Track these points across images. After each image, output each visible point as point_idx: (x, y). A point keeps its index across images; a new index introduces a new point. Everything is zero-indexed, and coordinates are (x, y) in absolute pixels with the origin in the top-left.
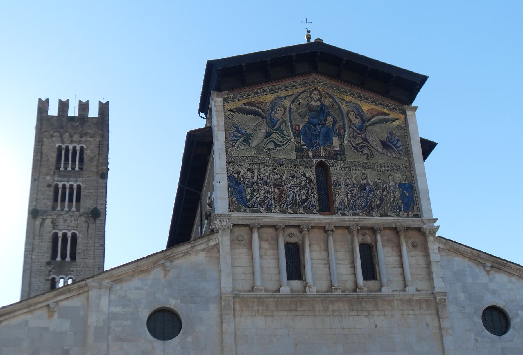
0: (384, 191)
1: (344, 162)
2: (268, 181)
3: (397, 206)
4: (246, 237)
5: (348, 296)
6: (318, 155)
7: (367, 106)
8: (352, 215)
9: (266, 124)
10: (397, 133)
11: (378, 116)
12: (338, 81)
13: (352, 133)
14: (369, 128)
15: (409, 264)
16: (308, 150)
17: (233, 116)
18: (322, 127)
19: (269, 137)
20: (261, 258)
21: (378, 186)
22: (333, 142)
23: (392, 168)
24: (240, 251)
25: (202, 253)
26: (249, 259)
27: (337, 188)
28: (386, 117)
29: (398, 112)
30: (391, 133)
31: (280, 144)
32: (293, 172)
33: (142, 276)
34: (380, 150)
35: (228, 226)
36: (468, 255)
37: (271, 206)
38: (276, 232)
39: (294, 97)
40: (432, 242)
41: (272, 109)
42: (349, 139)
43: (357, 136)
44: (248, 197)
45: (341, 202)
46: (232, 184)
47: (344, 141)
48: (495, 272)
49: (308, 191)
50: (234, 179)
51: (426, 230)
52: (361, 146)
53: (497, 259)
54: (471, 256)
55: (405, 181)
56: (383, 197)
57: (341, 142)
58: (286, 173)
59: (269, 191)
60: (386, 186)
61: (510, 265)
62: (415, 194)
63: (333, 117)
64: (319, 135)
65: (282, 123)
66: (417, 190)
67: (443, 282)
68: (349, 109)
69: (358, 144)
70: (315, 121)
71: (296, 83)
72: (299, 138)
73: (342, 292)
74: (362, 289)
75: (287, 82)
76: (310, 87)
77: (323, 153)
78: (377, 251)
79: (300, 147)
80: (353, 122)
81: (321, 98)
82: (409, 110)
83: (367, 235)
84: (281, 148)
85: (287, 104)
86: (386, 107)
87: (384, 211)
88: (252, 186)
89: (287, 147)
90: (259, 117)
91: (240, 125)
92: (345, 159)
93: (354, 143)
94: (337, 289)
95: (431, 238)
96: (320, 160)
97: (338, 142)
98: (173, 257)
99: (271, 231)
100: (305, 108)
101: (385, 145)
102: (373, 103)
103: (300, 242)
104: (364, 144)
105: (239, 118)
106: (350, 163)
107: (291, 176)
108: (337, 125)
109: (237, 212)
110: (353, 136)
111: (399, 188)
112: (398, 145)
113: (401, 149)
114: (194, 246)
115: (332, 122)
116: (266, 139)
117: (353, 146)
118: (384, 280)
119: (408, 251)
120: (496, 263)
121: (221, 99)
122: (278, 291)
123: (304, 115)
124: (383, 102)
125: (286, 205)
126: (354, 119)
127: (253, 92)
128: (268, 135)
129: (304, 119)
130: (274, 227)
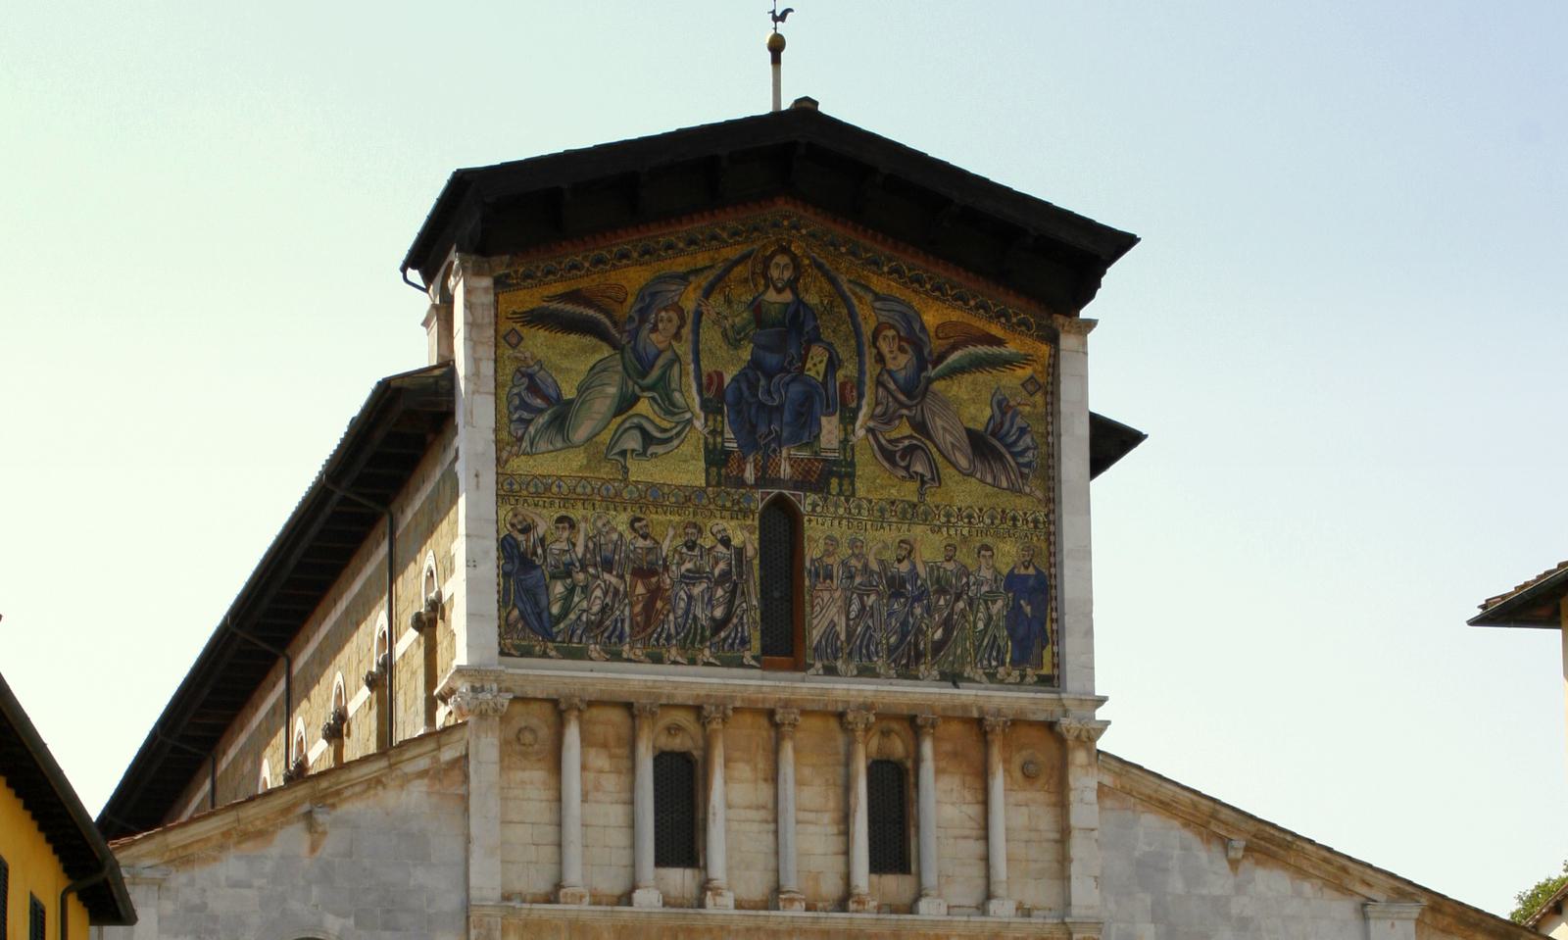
0: (958, 598)
1: (847, 501)
2: (617, 557)
3: (993, 647)
4: (545, 733)
5: (823, 920)
6: (773, 475)
7: (937, 310)
8: (855, 672)
9: (620, 368)
10: (1024, 404)
11: (970, 347)
13: (882, 403)
14: (938, 386)
15: (1007, 829)
16: (744, 458)
17: (522, 339)
18: (793, 380)
19: (627, 411)
20: (585, 799)
21: (943, 582)
22: (817, 437)
23: (992, 523)
24: (526, 775)
25: (418, 782)
26: (547, 800)
27: (819, 587)
28: (995, 350)
30: (1005, 403)
31: (658, 435)
32: (693, 530)
33: (247, 846)
34: (963, 463)
35: (495, 704)
36: (1183, 811)
37: (621, 638)
38: (629, 720)
39: (711, 275)
40: (1081, 766)
41: (643, 313)
42: (871, 424)
43: (897, 414)
44: (555, 610)
45: (828, 630)
46: (509, 567)
47: (856, 428)
48: (1258, 863)
49: (733, 593)
50: (515, 551)
51: (1068, 731)
52: (908, 446)
53: (1268, 829)
54: (1192, 815)
55: (1027, 568)
56: (956, 617)
57: (846, 434)
58: (671, 533)
59: (616, 592)
60: (968, 583)
61: (1303, 848)
62: (1052, 609)
63: (829, 347)
64: (780, 409)
65: (669, 365)
66: (1058, 598)
67: (1097, 892)
68: (882, 319)
69: (898, 440)
70: (772, 359)
71: (724, 229)
72: (719, 418)
73: (808, 909)
74: (864, 904)
75: (696, 225)
76: (765, 241)
77: (788, 470)
78: (917, 785)
79: (719, 446)
80: (891, 366)
81: (796, 280)
82: (1069, 332)
83: (893, 736)
84: (660, 450)
85: (690, 301)
86: (998, 317)
87: (953, 663)
88: (569, 575)
89: (678, 446)
90: (600, 343)
91: (541, 368)
92: (853, 489)
93: (884, 437)
94: (792, 901)
95: (1080, 757)
96: (777, 491)
97: (836, 432)
98: (338, 793)
99: (617, 716)
100: (745, 315)
101: (984, 447)
102: (960, 303)
103: (697, 753)
104: (915, 442)
105: (539, 343)
106: (865, 504)
107: (685, 544)
108: (840, 374)
109: (522, 656)
110: (884, 414)
111: (1005, 590)
112: (1021, 445)
113: (1026, 460)
114: (395, 764)
115: (823, 365)
116: (619, 419)
117: (881, 447)
118: (930, 878)
119: (1008, 790)
120: (1263, 839)
121: (486, 282)
122: (626, 899)
123: (738, 337)
124: (989, 302)
125: (664, 636)
126: (892, 356)
127: (585, 258)
128: (625, 404)
129: (740, 352)
130: (628, 706)
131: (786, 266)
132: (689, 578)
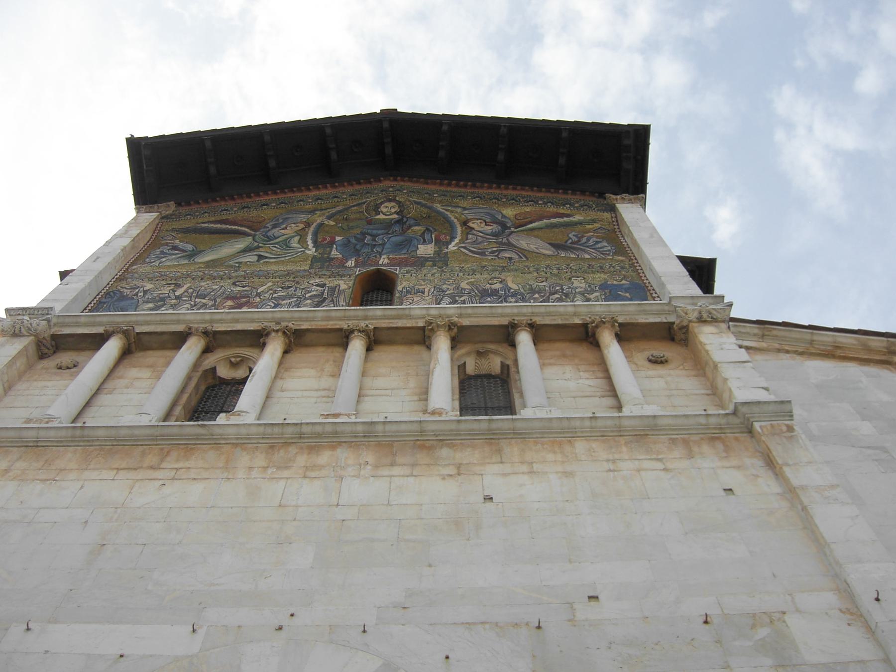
12: (441, 184)
28: (566, 219)
29: (594, 209)
35: (31, 324)
131: (393, 207)
132: (279, 298)
